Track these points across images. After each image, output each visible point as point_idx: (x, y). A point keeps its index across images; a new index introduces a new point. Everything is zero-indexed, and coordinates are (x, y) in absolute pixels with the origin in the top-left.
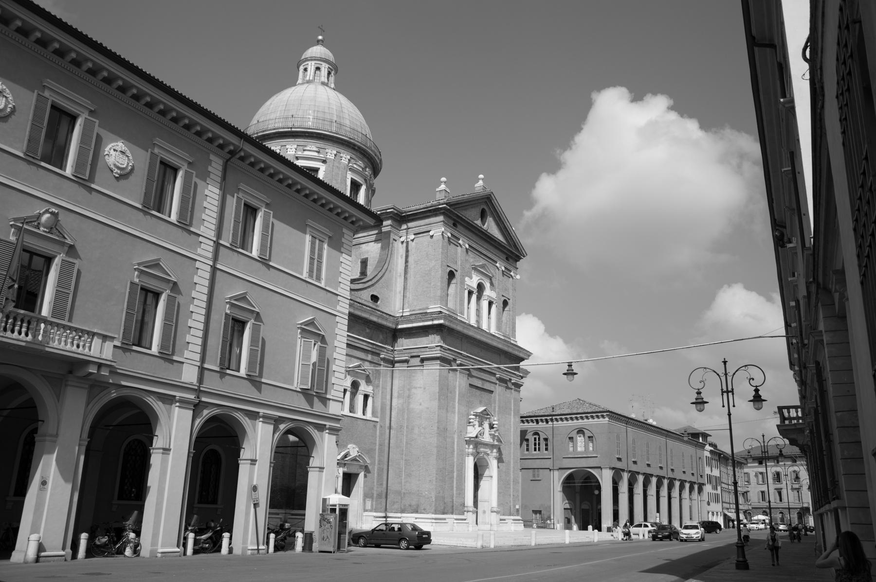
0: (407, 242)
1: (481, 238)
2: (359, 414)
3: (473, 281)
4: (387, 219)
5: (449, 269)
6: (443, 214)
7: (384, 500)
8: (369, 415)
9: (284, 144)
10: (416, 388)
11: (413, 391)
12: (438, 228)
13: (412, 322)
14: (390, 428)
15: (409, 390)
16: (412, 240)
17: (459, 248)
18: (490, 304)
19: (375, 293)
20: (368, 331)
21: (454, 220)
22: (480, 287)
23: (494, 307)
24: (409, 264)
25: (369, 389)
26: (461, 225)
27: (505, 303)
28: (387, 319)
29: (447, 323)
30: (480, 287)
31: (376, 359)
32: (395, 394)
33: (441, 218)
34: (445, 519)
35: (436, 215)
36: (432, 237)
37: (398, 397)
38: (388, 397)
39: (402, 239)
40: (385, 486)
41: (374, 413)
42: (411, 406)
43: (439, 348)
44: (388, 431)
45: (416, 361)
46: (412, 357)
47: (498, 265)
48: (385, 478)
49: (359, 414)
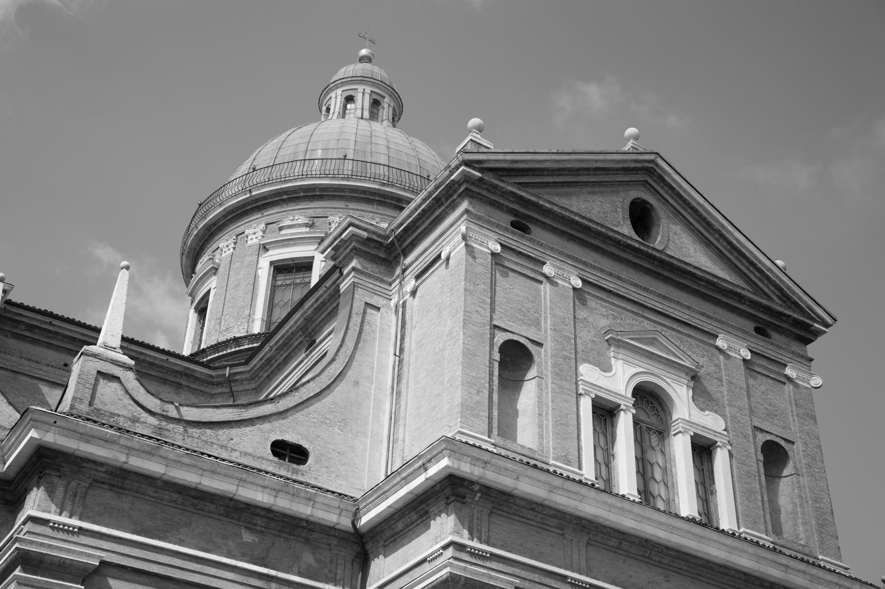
1: (636, 267)
3: (619, 378)
4: (348, 259)
6: (468, 194)
12: (459, 239)
16: (414, 293)
17: (546, 288)
18: (703, 450)
19: (291, 437)
20: (247, 537)
22: (648, 398)
23: (721, 458)
26: (536, 222)
27: (774, 455)
28: (309, 499)
29: (466, 469)
30: (648, 398)
35: (453, 206)
36: (448, 259)
43: (450, 552)
47: (719, 343)
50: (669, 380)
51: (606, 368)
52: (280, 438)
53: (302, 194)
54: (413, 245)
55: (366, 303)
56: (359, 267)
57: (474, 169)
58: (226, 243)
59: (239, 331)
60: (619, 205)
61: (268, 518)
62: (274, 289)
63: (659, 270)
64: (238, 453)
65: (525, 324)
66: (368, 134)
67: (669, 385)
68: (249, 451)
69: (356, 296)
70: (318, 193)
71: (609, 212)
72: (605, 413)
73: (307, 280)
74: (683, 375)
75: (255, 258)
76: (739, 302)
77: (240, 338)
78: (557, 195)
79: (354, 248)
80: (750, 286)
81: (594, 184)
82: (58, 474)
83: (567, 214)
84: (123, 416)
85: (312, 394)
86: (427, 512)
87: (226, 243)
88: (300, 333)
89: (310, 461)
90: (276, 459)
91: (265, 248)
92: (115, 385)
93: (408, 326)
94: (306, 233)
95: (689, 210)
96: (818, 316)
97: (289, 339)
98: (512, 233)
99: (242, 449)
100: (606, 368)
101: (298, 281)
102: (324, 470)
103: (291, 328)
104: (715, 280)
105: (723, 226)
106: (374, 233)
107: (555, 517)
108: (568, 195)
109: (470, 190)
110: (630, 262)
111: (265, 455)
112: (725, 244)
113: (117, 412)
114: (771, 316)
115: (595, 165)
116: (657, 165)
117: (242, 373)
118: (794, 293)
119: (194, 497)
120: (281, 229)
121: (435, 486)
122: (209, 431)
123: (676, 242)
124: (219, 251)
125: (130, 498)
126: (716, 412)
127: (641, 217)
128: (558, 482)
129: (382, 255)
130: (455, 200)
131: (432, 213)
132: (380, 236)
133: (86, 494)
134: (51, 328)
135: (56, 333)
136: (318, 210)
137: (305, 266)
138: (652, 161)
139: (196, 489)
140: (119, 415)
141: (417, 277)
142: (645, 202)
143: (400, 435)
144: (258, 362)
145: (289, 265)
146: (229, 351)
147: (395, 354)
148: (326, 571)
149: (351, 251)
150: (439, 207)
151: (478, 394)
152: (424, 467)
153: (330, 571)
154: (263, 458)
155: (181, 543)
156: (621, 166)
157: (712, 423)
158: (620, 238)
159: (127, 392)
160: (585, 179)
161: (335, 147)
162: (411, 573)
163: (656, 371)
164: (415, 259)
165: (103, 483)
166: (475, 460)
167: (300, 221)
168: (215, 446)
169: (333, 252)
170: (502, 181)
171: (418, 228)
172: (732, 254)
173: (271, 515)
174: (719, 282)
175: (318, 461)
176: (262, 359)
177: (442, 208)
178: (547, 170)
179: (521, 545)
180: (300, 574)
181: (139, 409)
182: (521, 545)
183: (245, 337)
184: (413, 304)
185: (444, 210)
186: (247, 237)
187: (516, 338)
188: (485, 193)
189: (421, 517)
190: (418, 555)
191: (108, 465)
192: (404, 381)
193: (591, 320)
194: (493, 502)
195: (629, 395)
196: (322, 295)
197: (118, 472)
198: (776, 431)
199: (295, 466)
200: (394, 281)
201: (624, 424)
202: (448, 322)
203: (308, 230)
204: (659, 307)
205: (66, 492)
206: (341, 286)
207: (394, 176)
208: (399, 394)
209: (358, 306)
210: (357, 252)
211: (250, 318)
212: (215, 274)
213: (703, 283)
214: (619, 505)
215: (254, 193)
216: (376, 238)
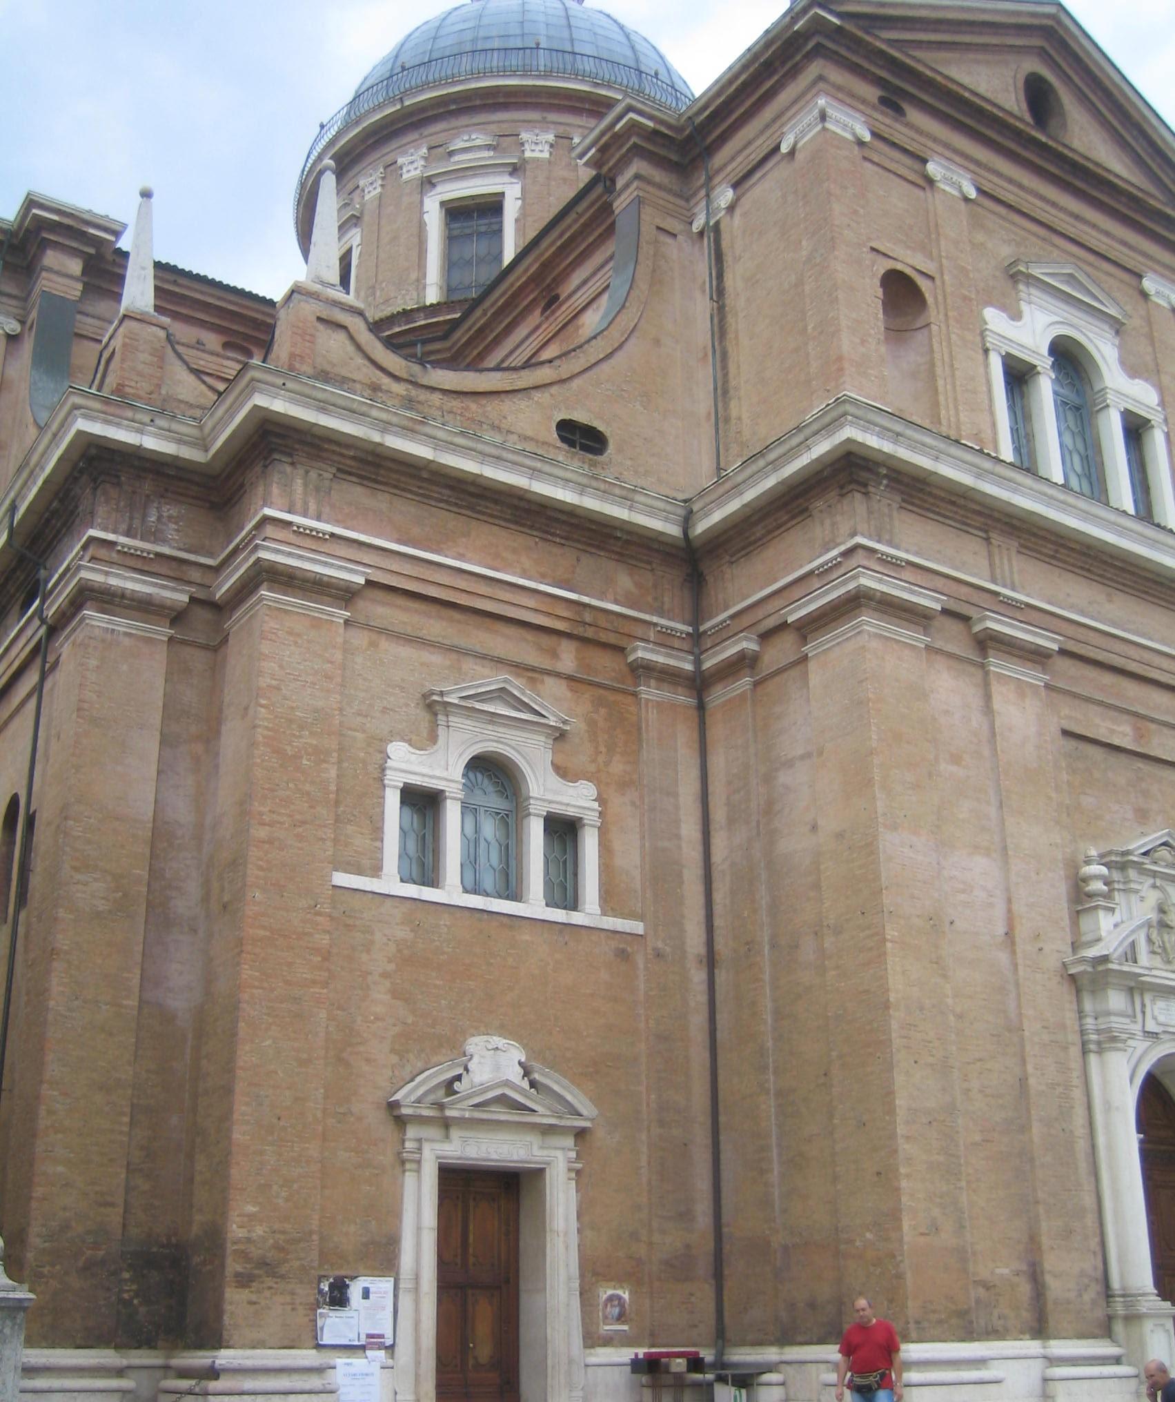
0: (717, 228)
2: (534, 905)
4: (624, 162)
5: (884, 266)
7: (708, 1290)
8: (590, 912)
9: (389, 159)
10: (790, 764)
11: (784, 778)
13: (737, 489)
14: (711, 961)
15: (768, 779)
16: (731, 208)
18: (1135, 430)
19: (580, 416)
21: (879, 82)
22: (1068, 357)
24: (729, 301)
25: (578, 798)
31: (605, 665)
32: (719, 814)
33: (816, 68)
34: (980, 1362)
36: (792, 153)
37: (731, 821)
38: (690, 829)
39: (697, 225)
40: (703, 1219)
41: (610, 900)
42: (785, 845)
44: (698, 977)
45: (781, 651)
46: (765, 637)
48: (703, 1185)
49: (534, 905)
50: (1091, 335)
51: (1016, 316)
52: (568, 417)
53: (478, 102)
54: (723, 139)
55: (659, 228)
56: (643, 172)
58: (370, 180)
59: (405, 303)
60: (1011, 81)
61: (571, 525)
62: (451, 239)
63: (1069, 178)
64: (515, 437)
65: (908, 247)
66: (563, 13)
68: (530, 433)
69: (643, 216)
70: (501, 100)
72: (1019, 376)
73: (495, 227)
74: (1106, 327)
75: (417, 197)
77: (412, 310)
79: (635, 145)
82: (289, 460)
84: (360, 382)
85: (601, 356)
86: (806, 509)
87: (370, 180)
88: (532, 286)
89: (611, 448)
90: (565, 446)
91: (428, 183)
92: (341, 336)
93: (728, 259)
94: (490, 158)
97: (515, 296)
98: (882, 113)
99: (520, 431)
100: (1016, 316)
101: (483, 229)
102: (629, 463)
103: (518, 279)
106: (662, 122)
107: (980, 513)
109: (823, 46)
113: (350, 375)
117: (438, 351)
119: (472, 494)
120: (451, 154)
121: (821, 471)
122: (473, 406)
123: (1085, 137)
124: (358, 191)
125: (387, 495)
128: (987, 465)
129: (674, 157)
130: (797, 64)
131: (758, 87)
132: (670, 126)
133: (330, 489)
134: (177, 290)
135: (183, 297)
136: (504, 126)
137: (491, 207)
139: (473, 483)
140: (354, 381)
141: (736, 186)
143: (734, 413)
144: (463, 335)
145: (467, 206)
146: (397, 329)
147: (711, 298)
148: (650, 599)
149: (629, 150)
150: (770, 76)
151: (863, 342)
152: (804, 445)
153: (655, 599)
154: (548, 444)
155: (460, 557)
159: (359, 347)
160: (967, 39)
161: (518, 32)
162: (785, 594)
163: (1075, 321)
164: (733, 155)
165: (350, 474)
167: (478, 142)
168: (485, 426)
169: (599, 155)
170: (868, 33)
171: (731, 112)
172: (1154, 160)
173: (573, 521)
175: (620, 450)
176: (470, 329)
177: (776, 78)
179: (939, 552)
180: (616, 602)
181: (378, 373)
182: (939, 552)
183: (418, 310)
184: (733, 228)
185: (777, 81)
186: (401, 168)
187: (899, 267)
188: (843, 52)
189: (793, 518)
190: (794, 570)
191: (357, 448)
192: (730, 336)
193: (990, 245)
194: (902, 493)
195: (1045, 350)
196: (569, 227)
197: (370, 458)
199: (591, 456)
200: (695, 194)
201: (1045, 388)
202: (804, 243)
203: (491, 153)
204: (1071, 231)
205: (305, 485)
206: (615, 205)
207: (606, 72)
208: (724, 356)
209: (648, 231)
210: (637, 151)
211: (420, 284)
212: (356, 225)
213: (1124, 199)
215: (407, 103)
216: (666, 132)
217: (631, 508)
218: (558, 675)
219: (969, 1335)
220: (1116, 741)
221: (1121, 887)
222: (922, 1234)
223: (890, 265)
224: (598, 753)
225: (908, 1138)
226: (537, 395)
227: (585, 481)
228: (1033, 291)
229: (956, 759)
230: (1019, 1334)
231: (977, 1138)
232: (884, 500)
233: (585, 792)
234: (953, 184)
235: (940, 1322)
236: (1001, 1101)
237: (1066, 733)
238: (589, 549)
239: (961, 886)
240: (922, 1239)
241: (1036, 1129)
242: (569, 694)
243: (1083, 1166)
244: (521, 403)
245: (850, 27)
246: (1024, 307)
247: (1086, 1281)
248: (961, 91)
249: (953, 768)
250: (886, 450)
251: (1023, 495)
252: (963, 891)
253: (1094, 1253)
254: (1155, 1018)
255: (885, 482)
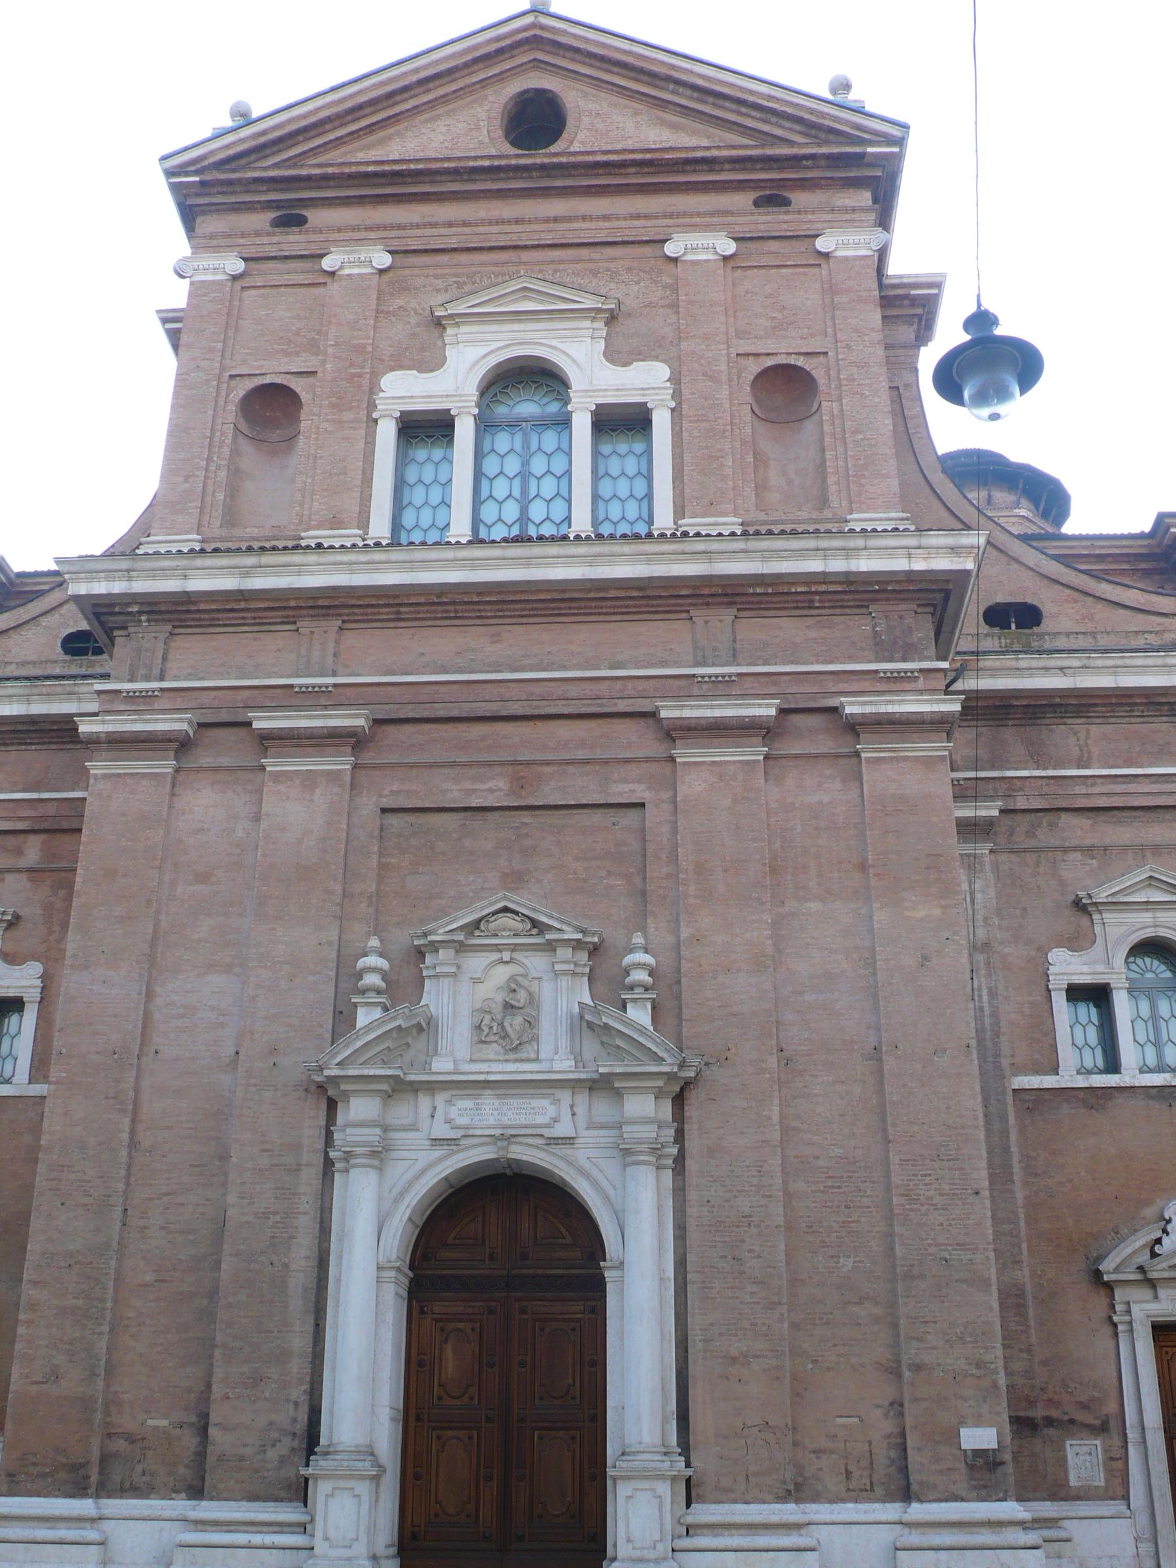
50: (554, 343)
52: (65, 632)
57: (187, 174)
64: (14, 666)
65: (287, 354)
67: (555, 348)
71: (469, 131)
74: (587, 324)
76: (711, 171)
78: (361, 149)
80: (751, 137)
81: (432, 104)
83: (354, 169)
95: (615, 69)
96: (876, 133)
104: (648, 156)
105: (673, 67)
108: (382, 142)
110: (490, 191)
111: (54, 657)
112: (689, 92)
114: (781, 169)
115: (415, 78)
116: (543, 27)
118: (823, 115)
123: (600, 124)
126: (656, 358)
127: (535, 120)
138: (533, 26)
142: (541, 92)
156: (469, 57)
157: (645, 381)
158: (453, 165)
163: (529, 336)
166: (110, 574)
172: (705, 102)
174: (658, 155)
178: (328, 120)
179: (223, 665)
182: (223, 665)
194: (169, 620)
198: (783, 349)
214: (363, 558)
217: (79, 700)
218: (18, 871)
219: (79, 1490)
220: (475, 802)
221: (431, 973)
222: (36, 1383)
223: (250, 384)
224: (51, 932)
225: (35, 1283)
226: (44, 621)
227: (27, 691)
228: (464, 329)
229: (202, 878)
230: (171, 1492)
231: (149, 1278)
232: (147, 638)
233: (31, 972)
234: (361, 263)
235: (44, 1475)
236: (191, 1237)
237: (384, 811)
238: (64, 746)
239: (182, 1011)
240: (35, 1388)
241: (227, 1266)
242: (28, 885)
243: (298, 1304)
244: (28, 633)
245: (208, 177)
246: (449, 351)
247: (276, 1435)
248: (363, 169)
249: (198, 888)
250: (116, 591)
251: (312, 573)
252: (182, 1016)
253: (296, 1404)
254: (448, 1121)
255: (143, 618)
